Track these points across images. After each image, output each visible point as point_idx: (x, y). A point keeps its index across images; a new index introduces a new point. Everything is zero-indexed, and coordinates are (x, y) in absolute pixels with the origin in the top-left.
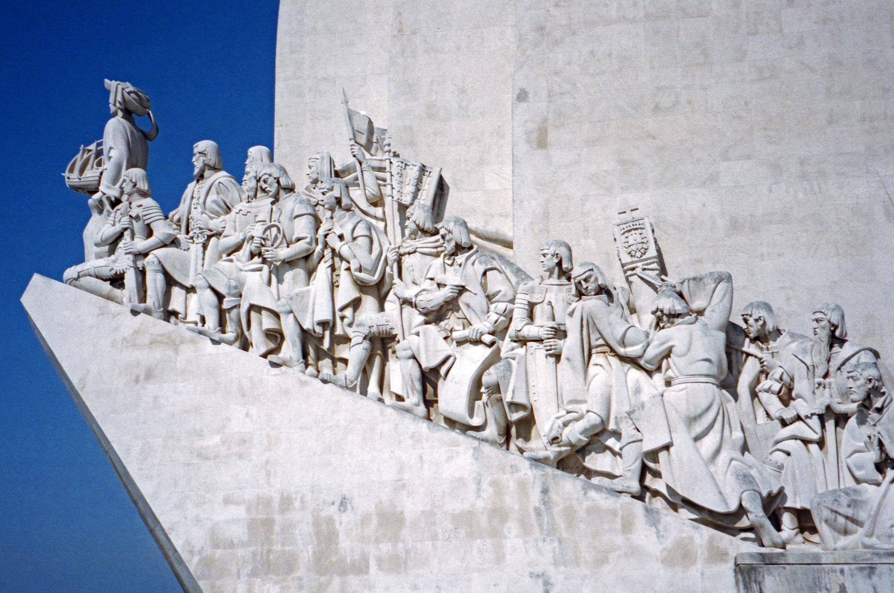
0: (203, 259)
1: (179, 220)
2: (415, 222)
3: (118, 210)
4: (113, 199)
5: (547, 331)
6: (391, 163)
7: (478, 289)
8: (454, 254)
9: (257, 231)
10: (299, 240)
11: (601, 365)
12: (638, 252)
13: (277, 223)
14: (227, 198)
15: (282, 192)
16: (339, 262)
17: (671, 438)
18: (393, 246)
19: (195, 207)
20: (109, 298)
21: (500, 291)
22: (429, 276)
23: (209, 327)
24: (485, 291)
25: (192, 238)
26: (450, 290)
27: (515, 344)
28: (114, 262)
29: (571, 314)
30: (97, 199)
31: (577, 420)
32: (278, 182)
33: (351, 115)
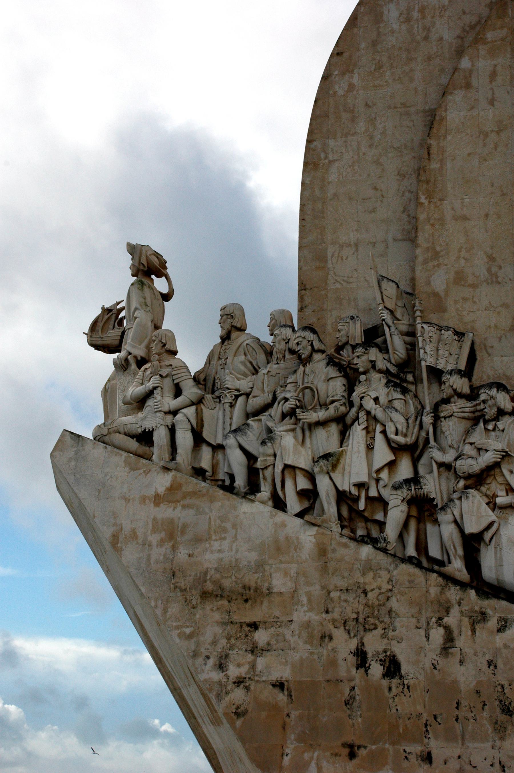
0: (231, 418)
1: (205, 380)
2: (452, 387)
3: (146, 369)
4: (139, 358)
10: (333, 402)
16: (374, 424)
25: (219, 397)
32: (312, 345)
33: (381, 279)
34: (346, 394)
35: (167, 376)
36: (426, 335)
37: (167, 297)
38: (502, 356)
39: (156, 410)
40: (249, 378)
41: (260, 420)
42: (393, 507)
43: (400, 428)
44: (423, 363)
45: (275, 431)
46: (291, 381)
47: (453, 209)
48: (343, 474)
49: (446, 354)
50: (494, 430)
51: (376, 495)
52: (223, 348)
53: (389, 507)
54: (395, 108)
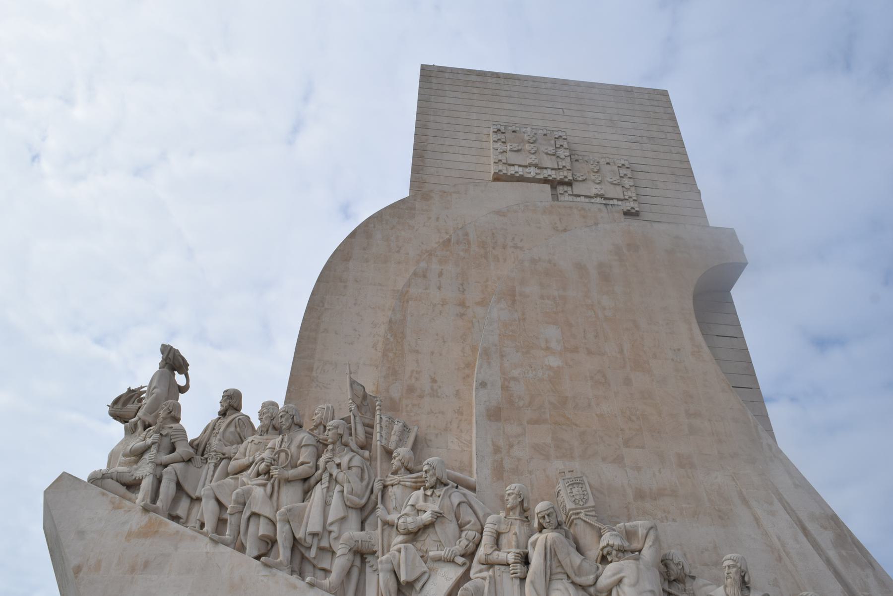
1: (198, 445)
3: (150, 430)
4: (147, 423)
6: (381, 418)
7: (451, 517)
8: (433, 487)
9: (266, 454)
10: (302, 464)
11: (560, 590)
13: (286, 449)
15: (293, 425)
18: (379, 478)
19: (214, 435)
20: (123, 497)
21: (469, 522)
22: (410, 503)
23: (207, 530)
24: (458, 521)
25: (206, 459)
26: (430, 515)
28: (136, 469)
29: (534, 544)
33: (353, 383)
34: (314, 460)
35: (166, 435)
36: (383, 424)
37: (183, 390)
38: (437, 448)
39: (150, 460)
40: (235, 446)
41: (238, 478)
45: (248, 484)
47: (409, 345)
48: (300, 522)
50: (431, 495)
51: (327, 545)
52: (219, 421)
53: (337, 556)
54: (375, 285)
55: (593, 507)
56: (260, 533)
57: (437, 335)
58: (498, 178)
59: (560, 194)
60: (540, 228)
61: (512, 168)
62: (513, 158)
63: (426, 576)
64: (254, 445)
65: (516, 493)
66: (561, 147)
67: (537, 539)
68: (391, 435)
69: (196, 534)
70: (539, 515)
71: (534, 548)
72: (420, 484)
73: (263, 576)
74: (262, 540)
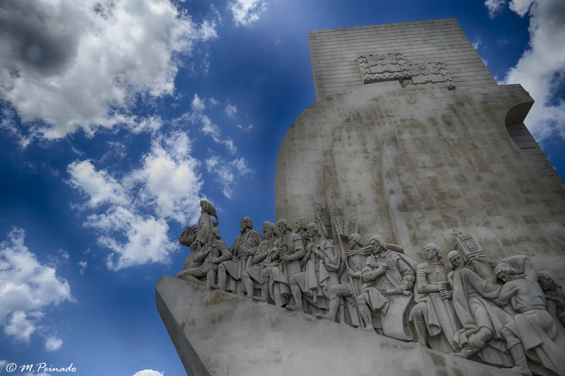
0: (245, 266)
1: (233, 250)
3: (205, 246)
4: (202, 243)
5: (442, 285)
6: (336, 219)
10: (298, 250)
11: (477, 303)
12: (473, 249)
14: (257, 240)
17: (542, 340)
18: (344, 253)
21: (407, 270)
24: (399, 270)
25: (240, 257)
27: (422, 295)
28: (202, 268)
29: (452, 277)
30: (195, 244)
31: (475, 333)
34: (303, 247)
35: (215, 247)
41: (260, 265)
42: (332, 299)
43: (332, 260)
44: (338, 233)
46: (276, 244)
47: (341, 178)
49: (348, 230)
51: (322, 295)
52: (242, 236)
53: (330, 300)
55: (482, 251)
56: (282, 292)
57: (356, 171)
58: (367, 82)
59: (406, 85)
60: (400, 103)
61: (374, 75)
62: (373, 69)
63: (387, 305)
64: (265, 246)
65: (432, 249)
66: (400, 59)
67: (453, 274)
68: (344, 228)
69: (245, 298)
70: (452, 259)
71: (453, 280)
72: (371, 252)
73: (289, 316)
74: (282, 296)
